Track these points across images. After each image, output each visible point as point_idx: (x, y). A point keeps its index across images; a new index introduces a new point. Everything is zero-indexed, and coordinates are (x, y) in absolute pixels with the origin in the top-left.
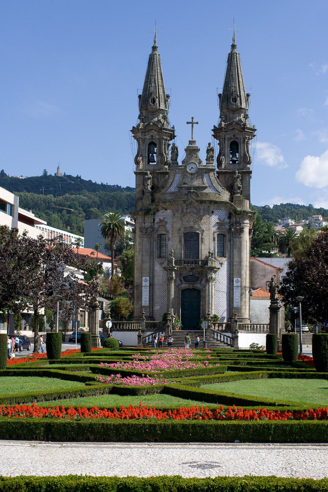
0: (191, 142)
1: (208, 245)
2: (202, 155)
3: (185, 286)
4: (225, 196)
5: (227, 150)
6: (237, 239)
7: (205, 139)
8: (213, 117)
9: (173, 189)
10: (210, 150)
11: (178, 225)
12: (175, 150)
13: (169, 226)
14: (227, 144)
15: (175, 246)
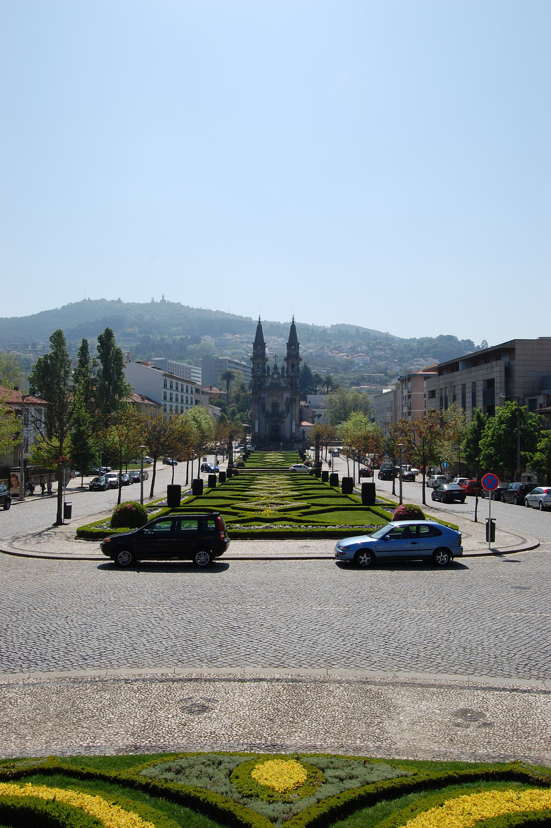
0: (276, 365)
1: (282, 408)
2: (280, 371)
3: (273, 424)
4: (290, 387)
5: (290, 368)
6: (294, 405)
7: (281, 364)
8: (284, 352)
9: (268, 385)
10: (283, 368)
11: (270, 399)
12: (268, 368)
13: (266, 400)
14: (290, 365)
15: (269, 408)
